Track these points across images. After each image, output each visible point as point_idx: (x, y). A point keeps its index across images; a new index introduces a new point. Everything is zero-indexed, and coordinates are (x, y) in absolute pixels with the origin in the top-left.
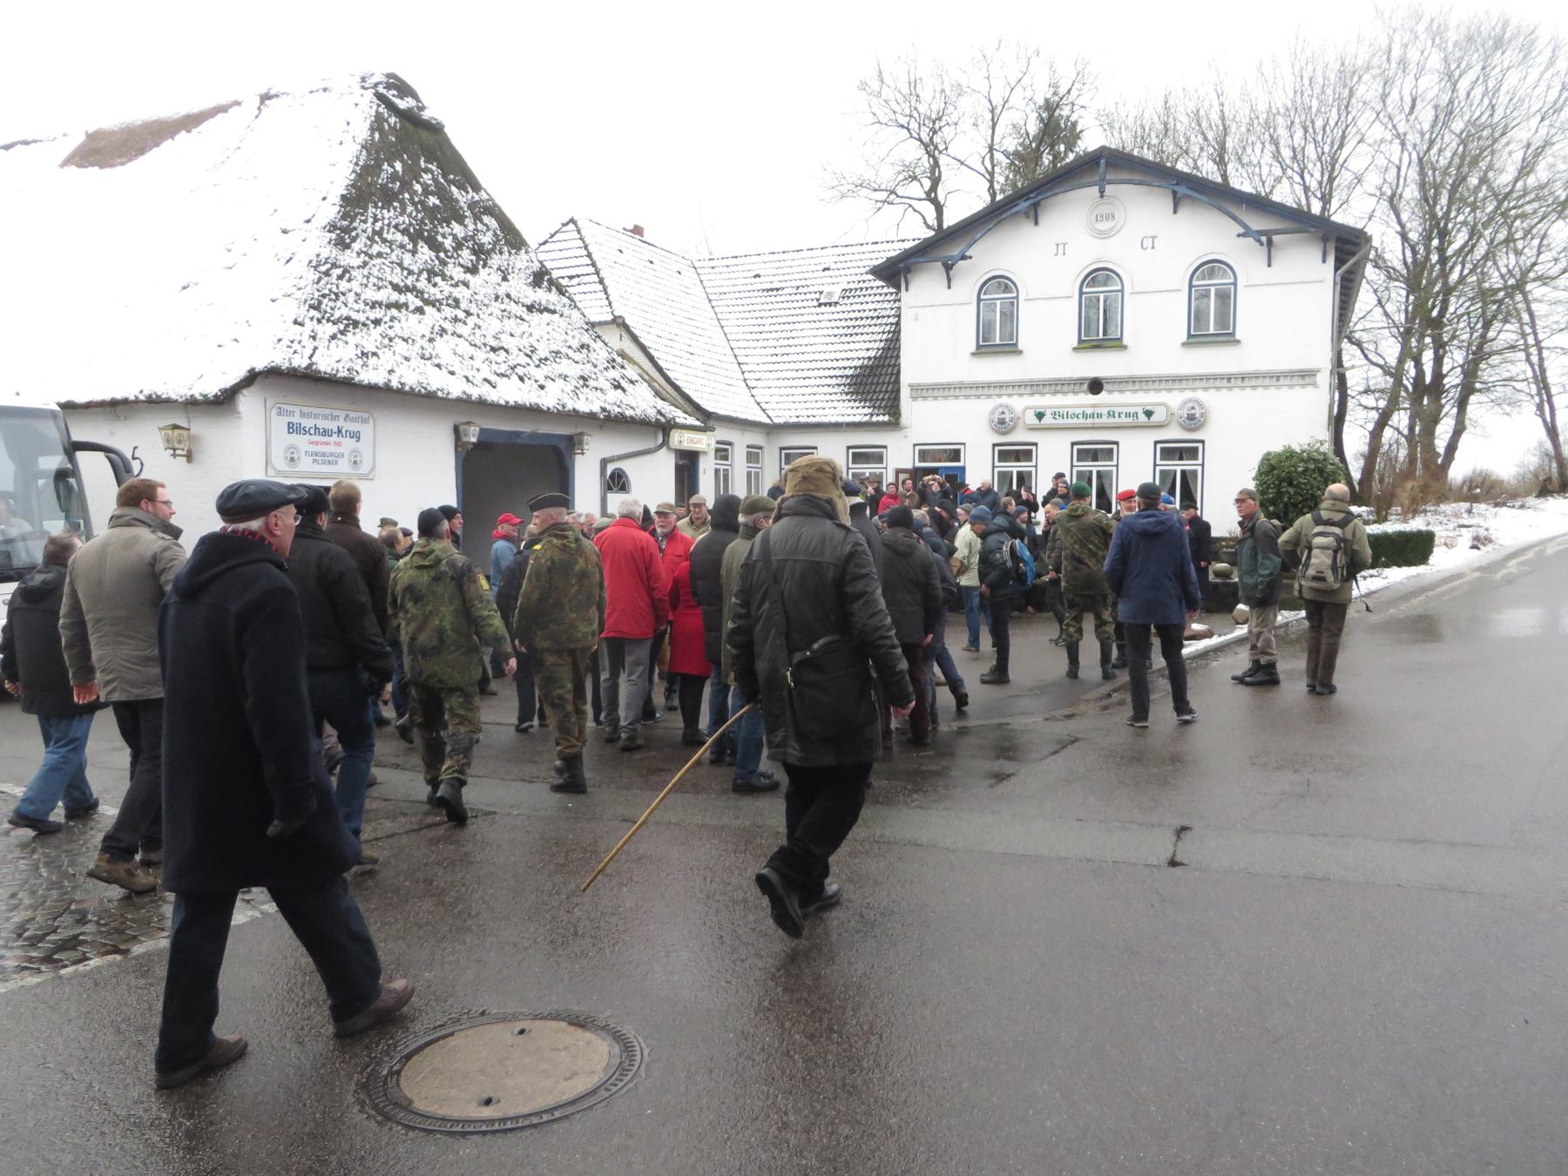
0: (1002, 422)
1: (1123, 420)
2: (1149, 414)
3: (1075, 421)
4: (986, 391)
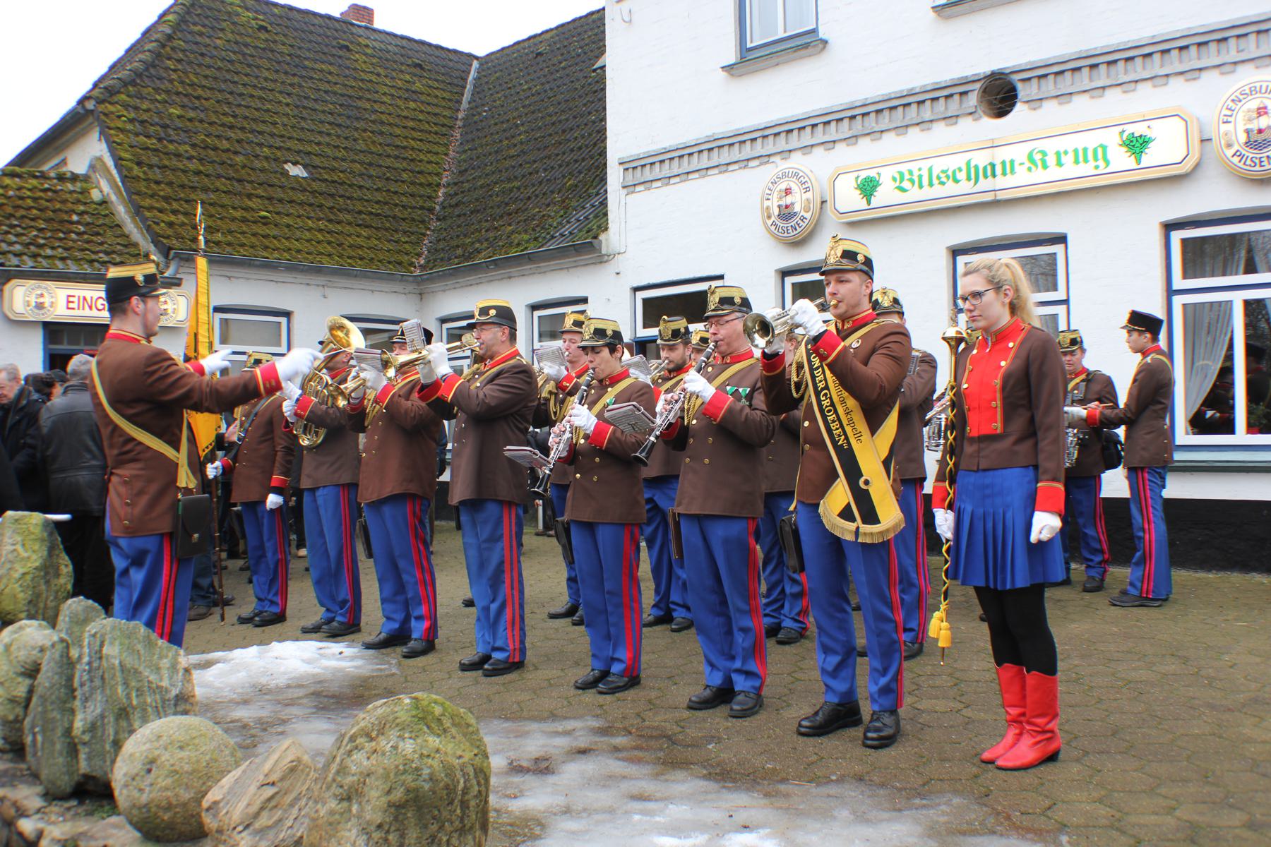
0: (786, 214)
1: (1071, 170)
2: (1137, 145)
3: (951, 188)
4: (759, 149)
